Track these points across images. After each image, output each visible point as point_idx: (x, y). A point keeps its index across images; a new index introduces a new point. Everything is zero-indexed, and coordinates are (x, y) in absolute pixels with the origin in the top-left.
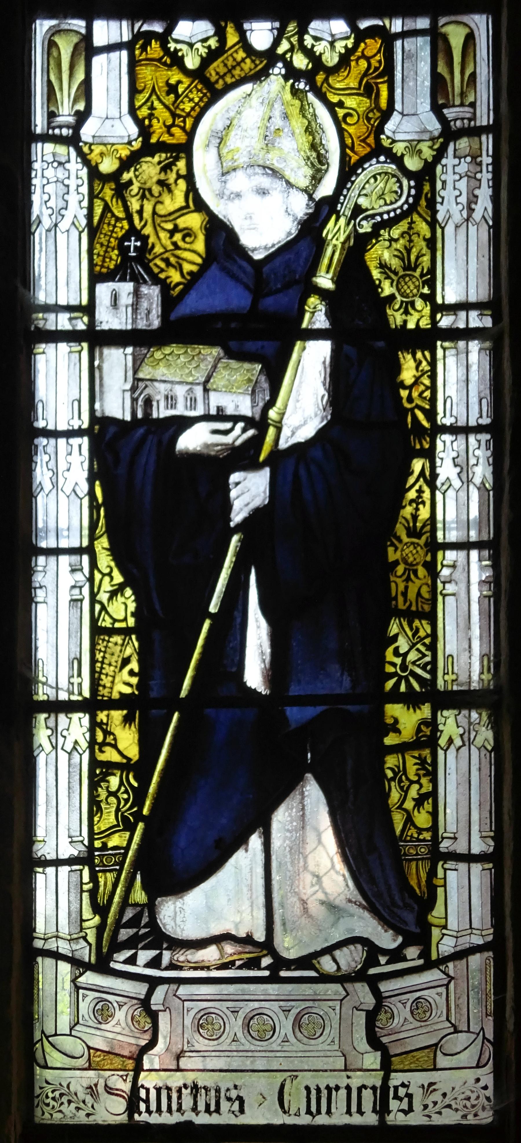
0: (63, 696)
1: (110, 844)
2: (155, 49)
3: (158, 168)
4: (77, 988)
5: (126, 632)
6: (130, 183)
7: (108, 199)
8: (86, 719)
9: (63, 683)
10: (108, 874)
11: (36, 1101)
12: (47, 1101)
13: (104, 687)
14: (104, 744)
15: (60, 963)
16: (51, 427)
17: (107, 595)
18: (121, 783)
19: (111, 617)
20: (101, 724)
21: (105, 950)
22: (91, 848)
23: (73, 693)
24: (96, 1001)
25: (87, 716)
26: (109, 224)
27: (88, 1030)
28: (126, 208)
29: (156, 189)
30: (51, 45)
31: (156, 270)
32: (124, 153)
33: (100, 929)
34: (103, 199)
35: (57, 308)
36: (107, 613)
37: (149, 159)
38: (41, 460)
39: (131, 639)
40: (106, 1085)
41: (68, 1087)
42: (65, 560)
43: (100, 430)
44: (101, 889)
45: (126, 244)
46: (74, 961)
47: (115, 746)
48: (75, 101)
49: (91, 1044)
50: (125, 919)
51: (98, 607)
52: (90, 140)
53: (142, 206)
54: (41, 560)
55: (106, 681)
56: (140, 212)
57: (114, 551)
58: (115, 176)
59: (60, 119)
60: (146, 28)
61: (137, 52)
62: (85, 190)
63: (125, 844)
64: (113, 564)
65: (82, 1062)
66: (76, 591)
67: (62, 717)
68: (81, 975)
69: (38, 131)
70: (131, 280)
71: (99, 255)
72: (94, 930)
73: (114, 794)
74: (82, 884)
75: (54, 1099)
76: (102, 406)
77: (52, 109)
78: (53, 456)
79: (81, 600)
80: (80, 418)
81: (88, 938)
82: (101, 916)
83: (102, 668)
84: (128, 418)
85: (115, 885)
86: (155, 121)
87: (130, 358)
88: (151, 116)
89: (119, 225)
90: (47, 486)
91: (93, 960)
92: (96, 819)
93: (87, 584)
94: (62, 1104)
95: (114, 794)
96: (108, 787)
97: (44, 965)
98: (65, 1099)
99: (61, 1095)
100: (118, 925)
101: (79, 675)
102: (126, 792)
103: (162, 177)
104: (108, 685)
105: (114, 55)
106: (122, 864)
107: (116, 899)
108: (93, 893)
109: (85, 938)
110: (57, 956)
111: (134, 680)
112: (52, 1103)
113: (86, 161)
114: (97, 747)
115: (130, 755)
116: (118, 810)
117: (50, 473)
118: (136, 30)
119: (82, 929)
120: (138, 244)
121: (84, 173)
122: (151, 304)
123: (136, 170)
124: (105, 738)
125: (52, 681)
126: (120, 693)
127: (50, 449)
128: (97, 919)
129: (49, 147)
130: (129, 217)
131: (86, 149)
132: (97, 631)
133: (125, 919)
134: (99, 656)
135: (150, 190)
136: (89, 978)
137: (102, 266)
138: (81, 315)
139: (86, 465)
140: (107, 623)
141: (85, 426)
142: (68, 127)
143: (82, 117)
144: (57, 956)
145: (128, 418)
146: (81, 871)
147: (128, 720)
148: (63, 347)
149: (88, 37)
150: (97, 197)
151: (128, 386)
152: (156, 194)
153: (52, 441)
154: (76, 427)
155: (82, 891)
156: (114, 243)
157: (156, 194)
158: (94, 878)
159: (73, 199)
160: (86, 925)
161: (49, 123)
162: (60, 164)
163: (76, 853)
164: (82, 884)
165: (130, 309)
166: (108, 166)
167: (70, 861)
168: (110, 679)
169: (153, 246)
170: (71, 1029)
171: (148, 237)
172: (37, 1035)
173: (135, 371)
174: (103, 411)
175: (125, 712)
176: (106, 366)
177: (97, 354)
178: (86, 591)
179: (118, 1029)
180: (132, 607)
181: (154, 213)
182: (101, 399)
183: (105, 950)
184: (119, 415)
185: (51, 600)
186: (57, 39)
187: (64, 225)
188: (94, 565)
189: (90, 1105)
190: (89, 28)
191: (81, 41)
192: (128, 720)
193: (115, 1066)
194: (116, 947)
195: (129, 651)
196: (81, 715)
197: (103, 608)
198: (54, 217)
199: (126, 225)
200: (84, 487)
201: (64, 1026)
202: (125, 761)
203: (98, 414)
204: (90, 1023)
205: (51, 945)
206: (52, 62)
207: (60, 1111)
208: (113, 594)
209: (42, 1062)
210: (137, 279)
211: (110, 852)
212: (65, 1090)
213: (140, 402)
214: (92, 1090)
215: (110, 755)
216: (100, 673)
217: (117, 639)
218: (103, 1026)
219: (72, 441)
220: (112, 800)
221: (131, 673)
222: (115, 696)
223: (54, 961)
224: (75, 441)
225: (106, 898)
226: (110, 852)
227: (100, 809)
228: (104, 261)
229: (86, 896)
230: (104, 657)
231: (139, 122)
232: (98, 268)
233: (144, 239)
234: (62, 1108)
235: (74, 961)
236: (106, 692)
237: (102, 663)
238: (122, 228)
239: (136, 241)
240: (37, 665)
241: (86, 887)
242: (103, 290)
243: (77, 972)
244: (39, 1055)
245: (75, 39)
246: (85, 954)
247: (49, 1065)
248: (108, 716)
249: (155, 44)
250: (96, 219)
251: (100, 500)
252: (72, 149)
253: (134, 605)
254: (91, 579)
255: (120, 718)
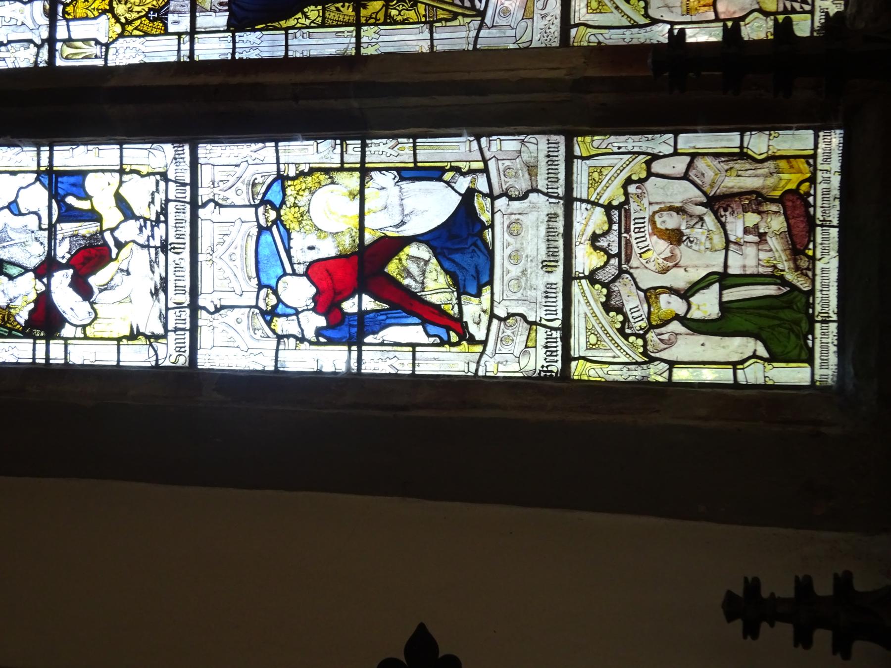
0: (353, 40)
1: (424, 13)
2: (69, 9)
3: (119, 5)
4: (493, 26)
5: (324, 10)
6: (125, 18)
7: (132, 28)
8: (365, 28)
9: (347, 40)
10: (438, 13)
11: (548, 46)
12: (549, 40)
13: (349, 19)
14: (376, 19)
15: (480, 36)
16: (231, 51)
17: (307, 20)
18: (395, 9)
19: (317, 18)
20: (367, 21)
21: (475, 13)
22: (425, 23)
23: (352, 35)
24: (500, 17)
25: (363, 28)
26: (143, 27)
27: (514, 20)
28: (137, 19)
29: (129, 5)
30: (67, 58)
31: (163, 3)
32: (113, 20)
33: (464, 16)
34: (132, 31)
35: (179, 50)
36: (315, 20)
37: (115, 9)
38: (245, 56)
39: (327, 7)
40: (542, 10)
41: (542, 29)
42: (290, 42)
43: (232, 27)
44: (445, 17)
45: (151, 19)
46: (479, 29)
47: (377, 13)
48: (91, 46)
49: (521, 18)
50: (460, 4)
51: (312, 25)
52: (107, 38)
53: (136, 12)
54: (290, 53)
55: (347, 18)
56: (138, 12)
57: (287, 18)
58: (123, 25)
59: (99, 54)
60: (61, 14)
61: (71, 17)
62: (128, 39)
63: (424, 6)
64: (293, 18)
65: (529, 22)
66: (305, 35)
67: (363, 40)
68: (486, 25)
69: (103, 63)
70: (167, 15)
71: (156, 31)
72: (465, 19)
73: (400, 12)
74: (442, 26)
75: (547, 36)
76: (222, 27)
77: (93, 57)
78: (244, 49)
79: (309, 33)
80: (227, 37)
81: (468, 22)
82: (458, 16)
83: (340, 21)
84: (227, 13)
85: (444, 9)
86: (100, 8)
87: (201, 14)
88: (98, 10)
89: (143, 22)
90: (257, 52)
91: (480, 19)
92: (411, 21)
93: (302, 30)
94: (550, 32)
95: (400, 12)
96: (397, 16)
97: (482, 44)
98: (548, 31)
99: (546, 33)
100: (463, 7)
101: (343, 32)
102: (399, 6)
103: (123, 2)
104: (348, 18)
105: (71, 28)
106: (433, 6)
107: (450, 8)
108: (447, 20)
109: (469, 23)
110: (477, 37)
111: (347, 4)
112: (549, 37)
113: (116, 39)
114: (377, 22)
115: (382, 5)
116: (407, 10)
117: (251, 50)
118: (62, 18)
119: (464, 25)
120: (152, 12)
121: (121, 40)
122: (178, 5)
123: (120, 16)
124: (373, 18)
125: (345, 46)
126: (352, 11)
127: (240, 51)
128: (460, 18)
129: (110, 57)
130: (140, 18)
131: (111, 40)
132: (323, 25)
133: (460, 4)
134: (335, 23)
135: (129, 8)
136: (488, 20)
137: (161, 29)
138: (182, 39)
139: (248, 33)
140: (320, 19)
141: (231, 34)
142: (101, 49)
143: (97, 42)
144: (477, 37)
145: (227, 13)
146: (436, 27)
147: (365, 7)
148: (196, 46)
149: (64, 41)
150: (131, 33)
151: (213, 14)
152: (131, 5)
153: (237, 50)
154: (231, 39)
155: (446, 26)
156: (151, 24)
157: (131, 5)
158: (440, 20)
159: (132, 45)
160: (462, 24)
161: (100, 58)
162: (117, 52)
163: (427, 30)
164: (442, 26)
165: (180, 15)
166: (118, 29)
167: (431, 33)
168: (346, 17)
169: (153, 5)
170: (513, 29)
171: (149, 8)
172: (516, 46)
173: (208, 11)
174: (224, 26)
175: (362, 9)
176: (205, 26)
177: (199, 30)
178: (305, 31)
179: (514, 5)
180: (313, 7)
181: (139, 6)
182: (219, 27)
183: (475, 13)
184: (227, 17)
185: (309, 48)
186: (64, 56)
187: (143, 49)
188: (293, 28)
189: (551, 18)
190: (60, 41)
191: (66, 44)
192: (365, 7)
193: (532, 5)
194: (473, 7)
195: (333, 8)
196: (362, 30)
197: (312, 22)
198: (140, 54)
199: (143, 19)
200: (258, 33)
201: (511, 33)
202: (384, 8)
203: (226, 28)
204: (510, 19)
205: (472, 40)
206: (74, 58)
207: (554, 33)
208: (307, 17)
209: (529, 43)
210: (166, 13)
211: (427, 13)
212: (543, 31)
213: (221, 8)
214: (543, 17)
215: (381, 16)
216: (343, 22)
217: (327, 15)
218: (512, 12)
219: (237, 41)
220: (402, 13)
221: (343, 6)
222: (353, 13)
223: (479, 39)
224: (237, 39)
225: (449, 14)
226: (427, 13)
227: (406, 19)
228: (159, 29)
229: (448, 24)
230: (336, 20)
231: (100, 14)
232: (162, 32)
233: (150, 9)
234: (552, 32)
235: (479, 29)
236: (352, 18)
237: (338, 21)
238: (145, 21)
239: (154, 14)
240: (338, 54)
241: (444, 24)
242: (172, 28)
243: (485, 26)
244: (525, 45)
245: (65, 47)
246: (476, 23)
247: (530, 39)
248: (363, 17)
249: (68, 9)
250: (141, 33)
251: (264, 25)
252: (111, 47)
253: (312, 6)
254: (300, 28)
255: (365, 10)
